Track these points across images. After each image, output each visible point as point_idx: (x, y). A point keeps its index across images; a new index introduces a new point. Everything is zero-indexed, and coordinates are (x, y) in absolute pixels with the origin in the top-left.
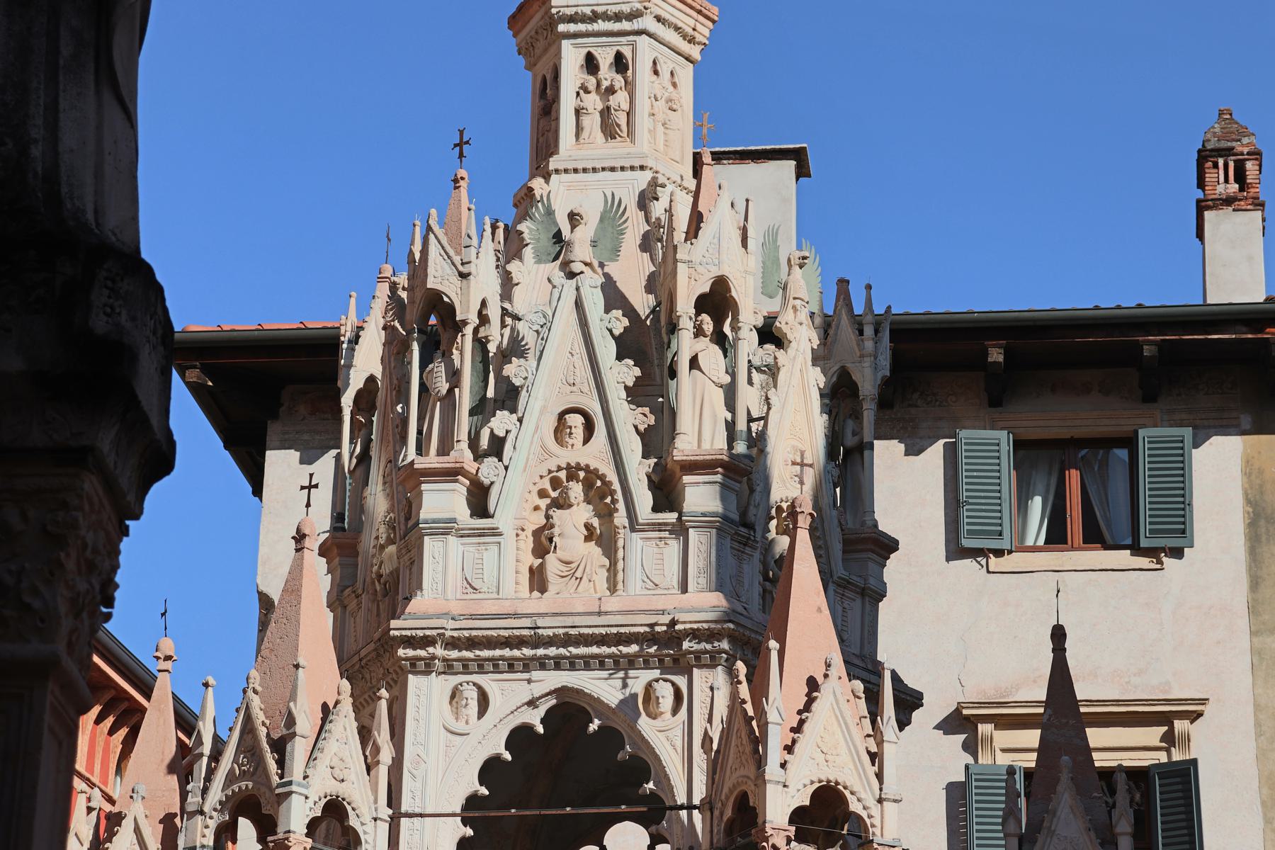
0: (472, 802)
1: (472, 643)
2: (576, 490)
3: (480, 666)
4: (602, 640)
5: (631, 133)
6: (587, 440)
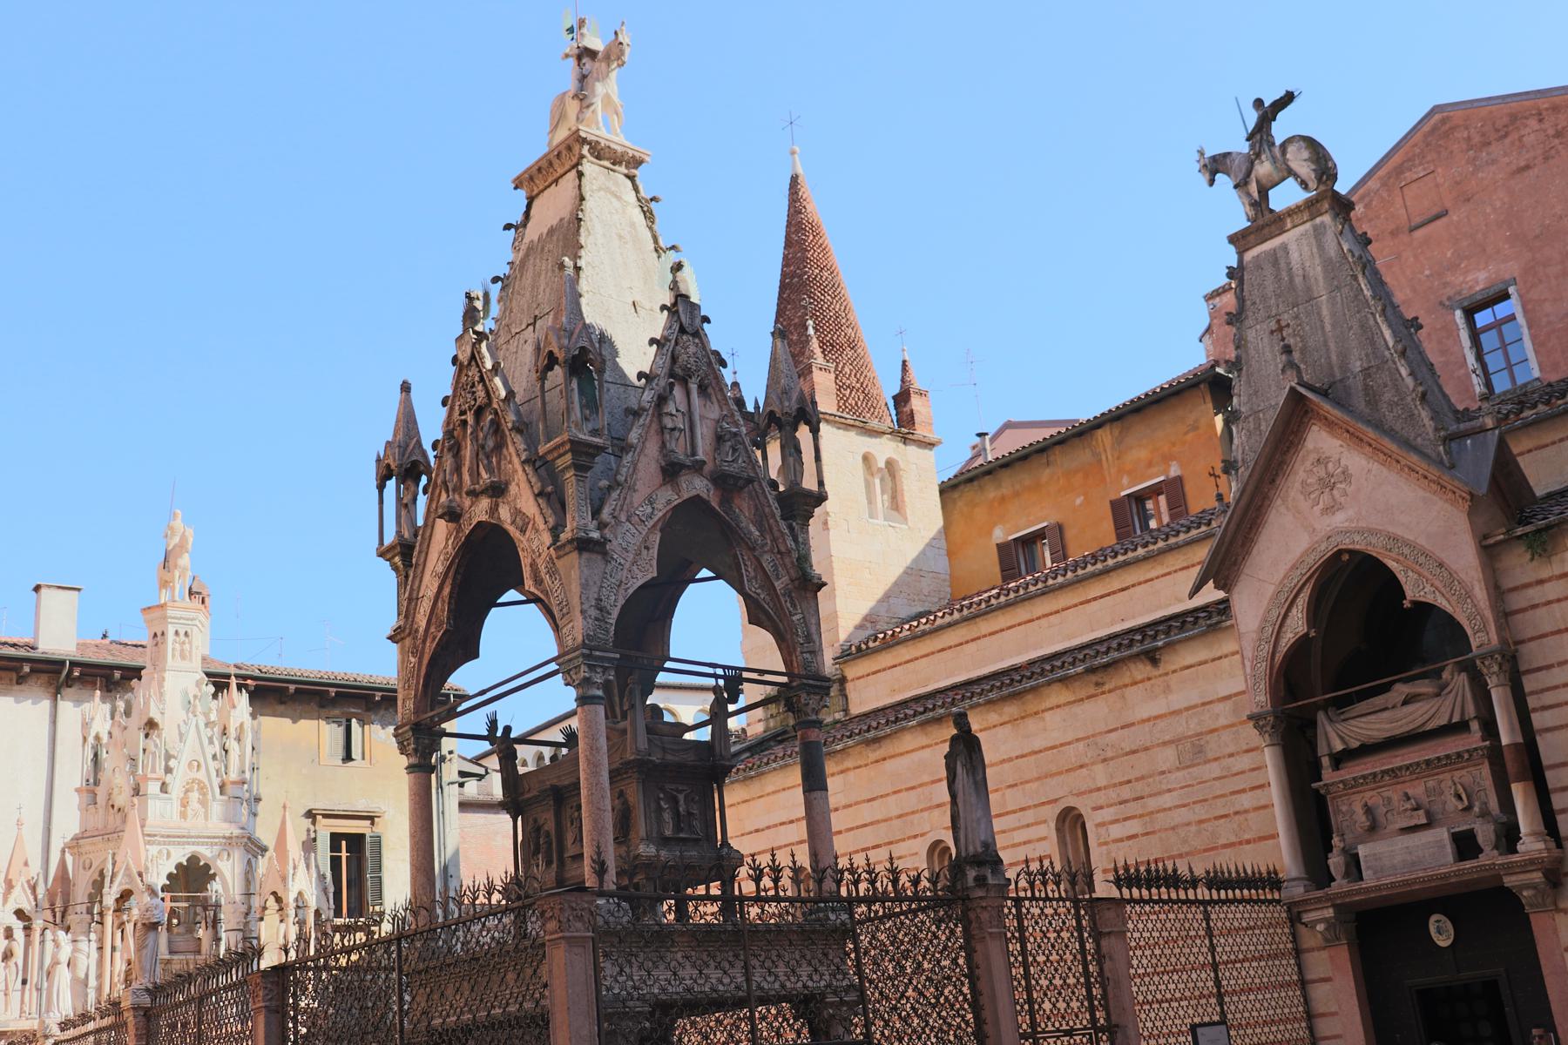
1: (168, 836)
3: (169, 844)
4: (208, 837)
5: (191, 660)
6: (198, 770)
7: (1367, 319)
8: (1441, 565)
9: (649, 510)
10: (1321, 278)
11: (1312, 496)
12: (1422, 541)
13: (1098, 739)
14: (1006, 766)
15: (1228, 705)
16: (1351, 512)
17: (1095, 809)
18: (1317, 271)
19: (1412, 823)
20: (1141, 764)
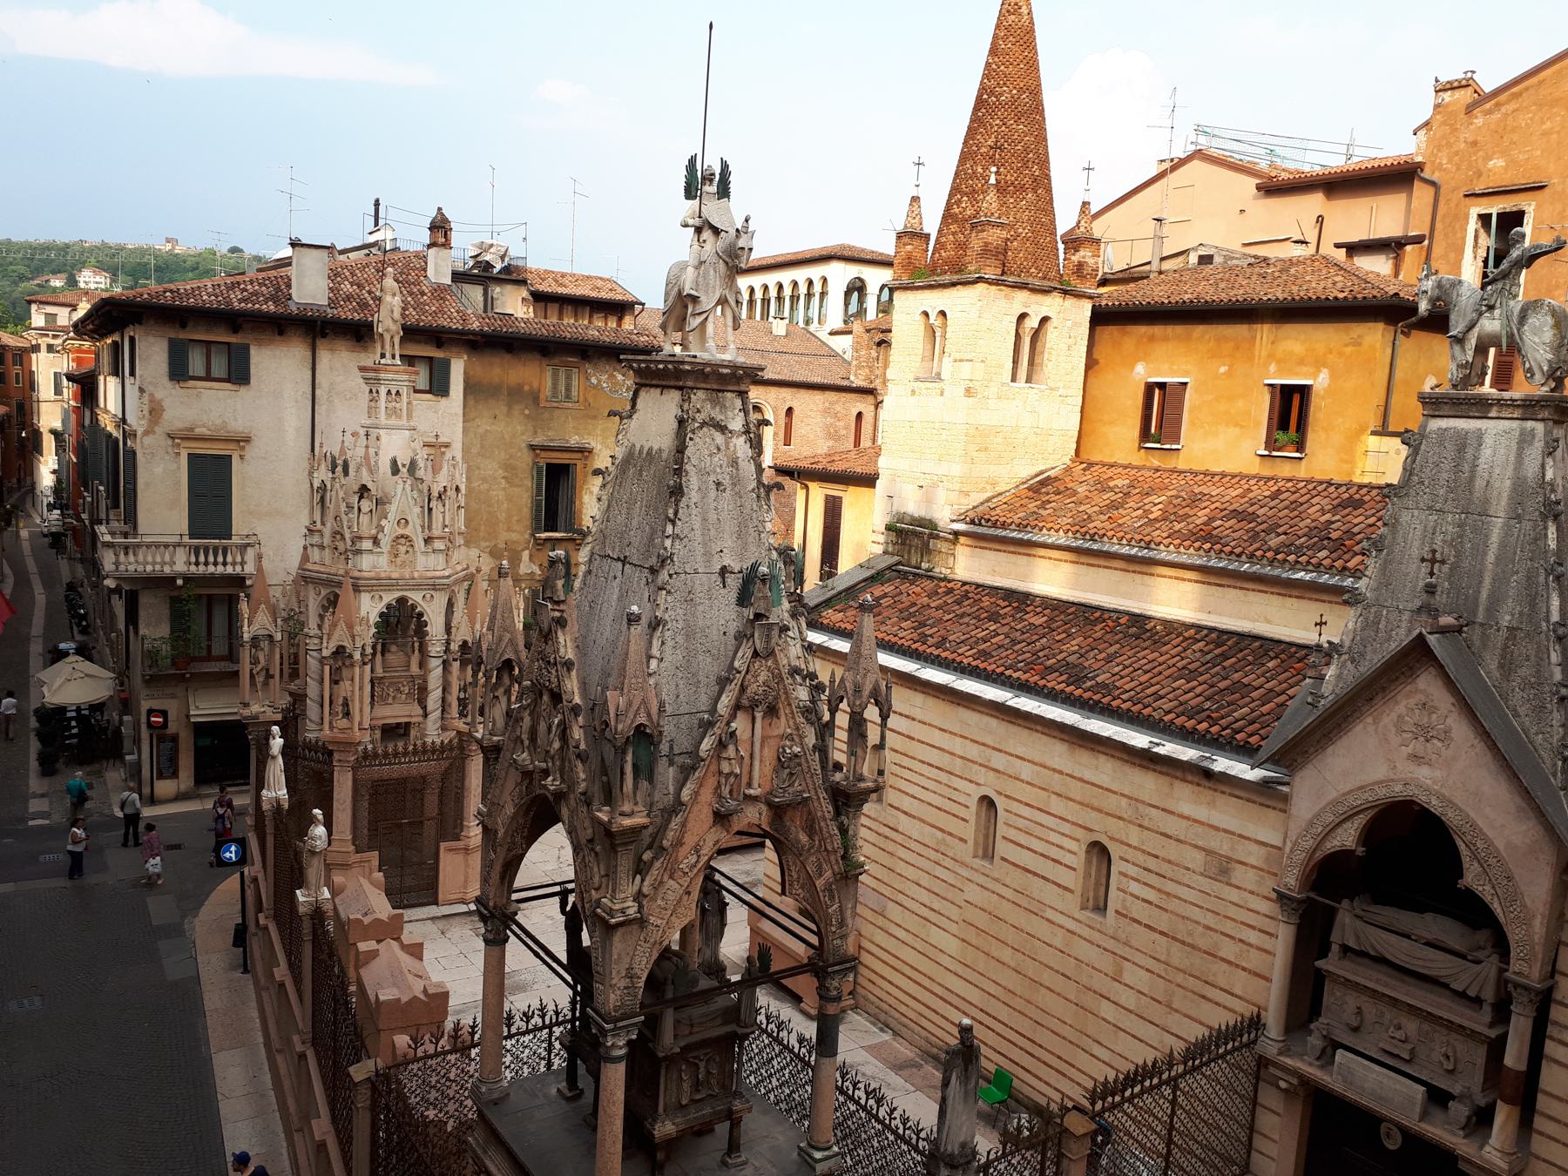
7: (1538, 575)
8: (1509, 879)
9: (693, 859)
10: (1505, 495)
11: (1405, 735)
12: (1500, 844)
13: (1141, 807)
14: (1057, 775)
15: (1263, 850)
16: (1438, 774)
17: (1122, 858)
18: (1504, 487)
19: (1396, 1052)
20: (1171, 851)
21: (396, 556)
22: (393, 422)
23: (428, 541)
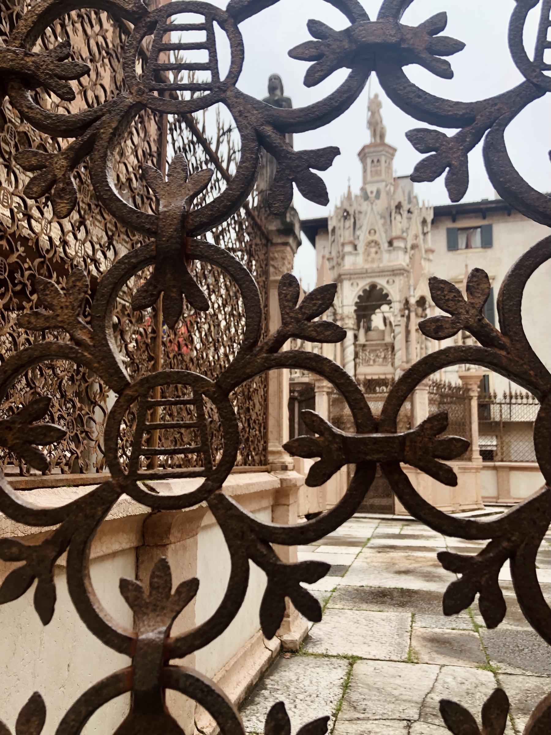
0: (357, 303)
2: (373, 244)
21: (368, 255)
22: (376, 178)
23: (390, 243)
